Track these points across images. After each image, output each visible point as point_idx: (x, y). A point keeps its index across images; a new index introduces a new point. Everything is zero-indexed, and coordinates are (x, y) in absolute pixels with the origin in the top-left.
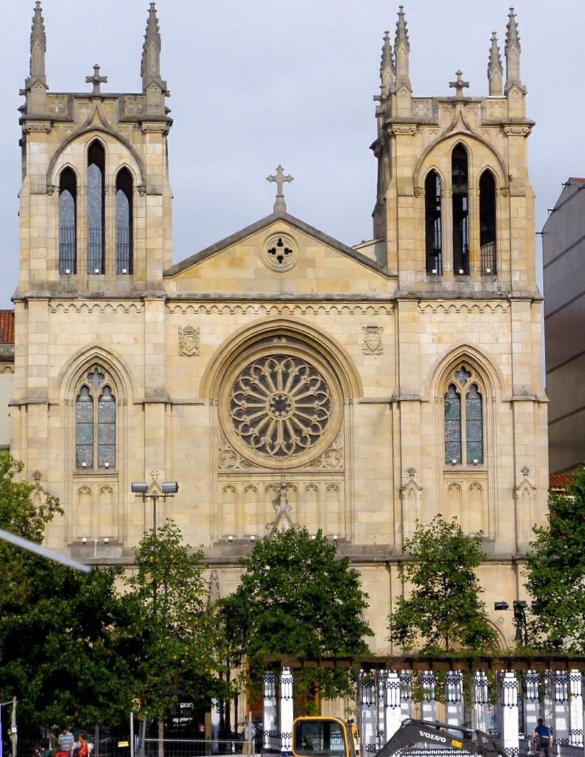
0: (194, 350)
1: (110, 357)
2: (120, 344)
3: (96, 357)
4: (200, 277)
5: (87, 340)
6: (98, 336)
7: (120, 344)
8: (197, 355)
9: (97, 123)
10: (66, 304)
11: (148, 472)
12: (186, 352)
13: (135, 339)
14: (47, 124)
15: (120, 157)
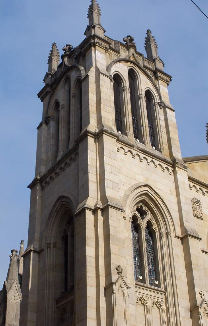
0: (201, 215)
1: (156, 197)
2: (161, 190)
3: (146, 194)
4: (195, 171)
5: (141, 180)
6: (147, 179)
7: (161, 190)
8: (202, 219)
9: (132, 59)
10: (127, 149)
11: (197, 291)
12: (197, 214)
13: (170, 191)
14: (107, 46)
15: (147, 84)
